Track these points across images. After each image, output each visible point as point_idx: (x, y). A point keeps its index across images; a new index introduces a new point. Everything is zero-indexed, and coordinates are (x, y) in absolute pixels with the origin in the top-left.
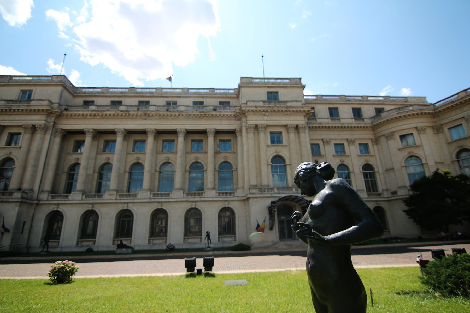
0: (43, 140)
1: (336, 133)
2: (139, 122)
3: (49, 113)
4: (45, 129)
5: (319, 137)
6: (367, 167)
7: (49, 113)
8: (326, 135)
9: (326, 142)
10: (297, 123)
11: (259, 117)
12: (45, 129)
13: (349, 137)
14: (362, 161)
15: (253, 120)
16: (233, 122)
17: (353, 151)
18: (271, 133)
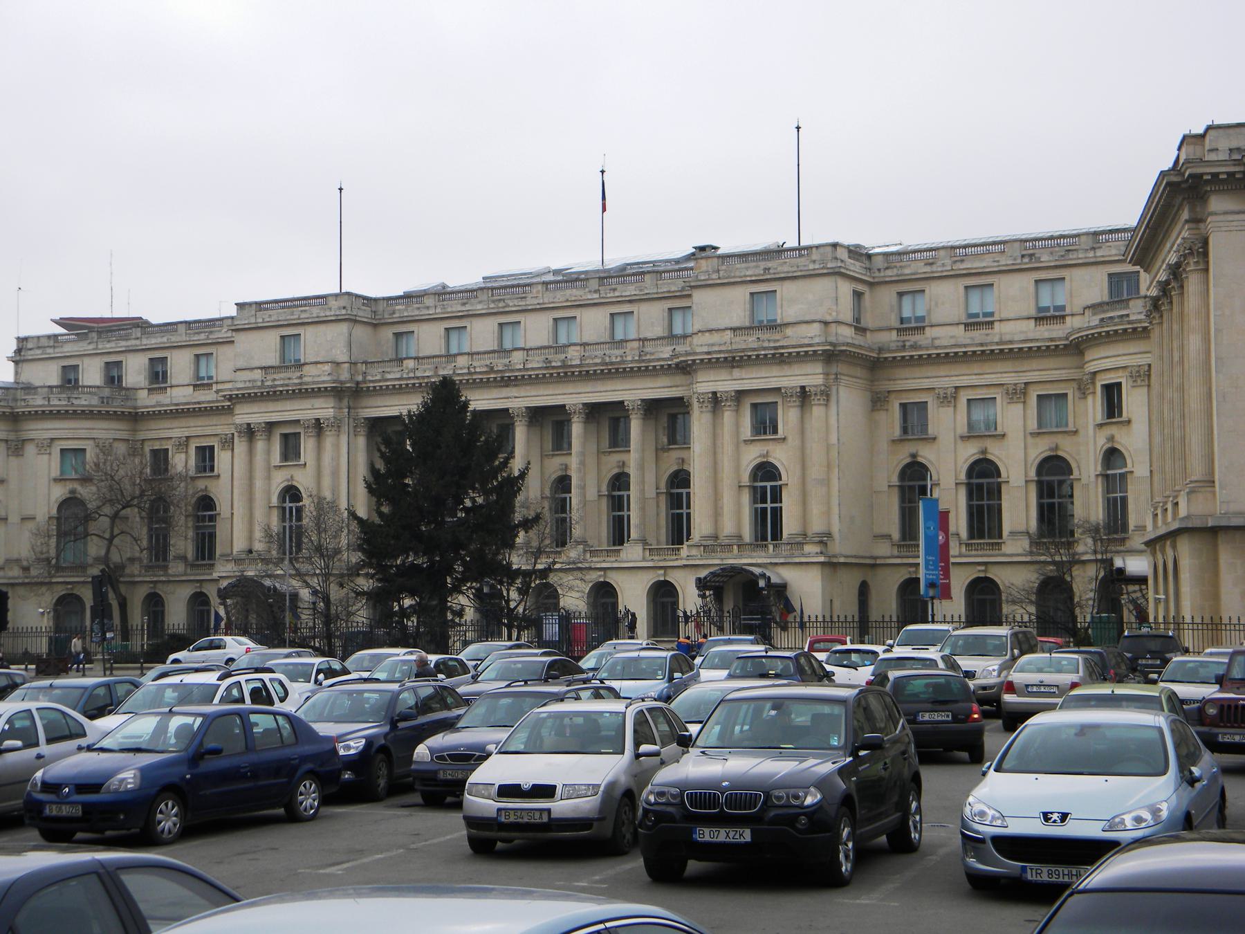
0: (337, 447)
1: (976, 368)
2: (495, 393)
3: (336, 392)
4: (337, 425)
5: (926, 383)
6: (1112, 455)
7: (336, 392)
8: (945, 378)
9: (949, 398)
10: (803, 381)
11: (723, 374)
12: (337, 425)
13: (1009, 379)
14: (1039, 449)
15: (708, 383)
16: (679, 379)
17: (1014, 419)
18: (754, 406)
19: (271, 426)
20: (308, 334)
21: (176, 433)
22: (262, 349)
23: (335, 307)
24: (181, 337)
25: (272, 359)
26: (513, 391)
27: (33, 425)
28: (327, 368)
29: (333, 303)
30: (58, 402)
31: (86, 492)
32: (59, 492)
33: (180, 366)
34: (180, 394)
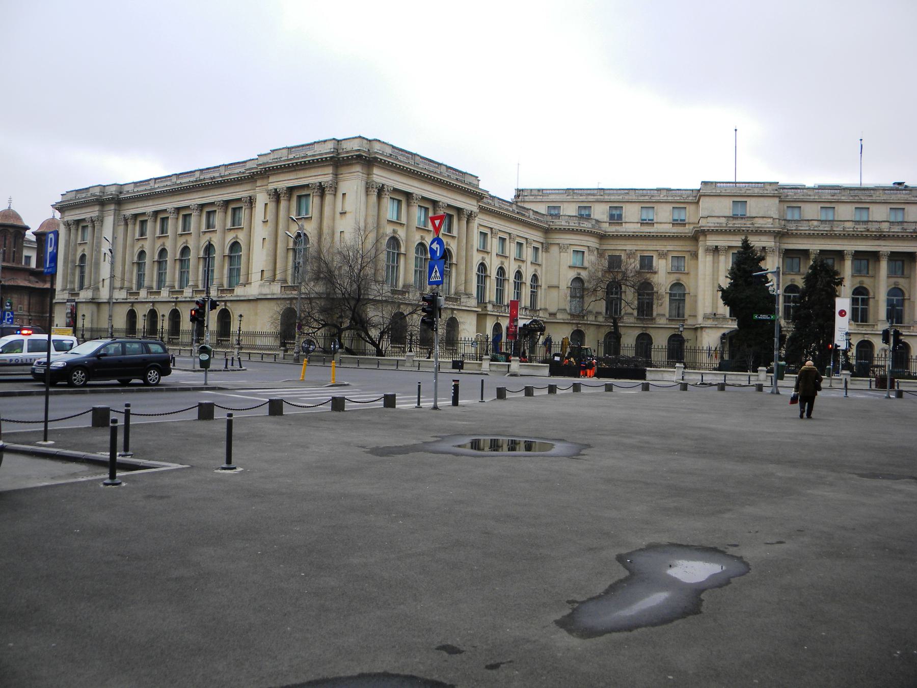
3: (780, 235)
19: (729, 247)
20: (751, 202)
21: (628, 248)
22: (724, 207)
23: (770, 190)
24: (633, 197)
25: (729, 213)
26: (882, 243)
27: (557, 236)
28: (770, 220)
29: (768, 187)
30: (573, 224)
31: (584, 274)
32: (572, 274)
33: (631, 213)
34: (631, 226)
